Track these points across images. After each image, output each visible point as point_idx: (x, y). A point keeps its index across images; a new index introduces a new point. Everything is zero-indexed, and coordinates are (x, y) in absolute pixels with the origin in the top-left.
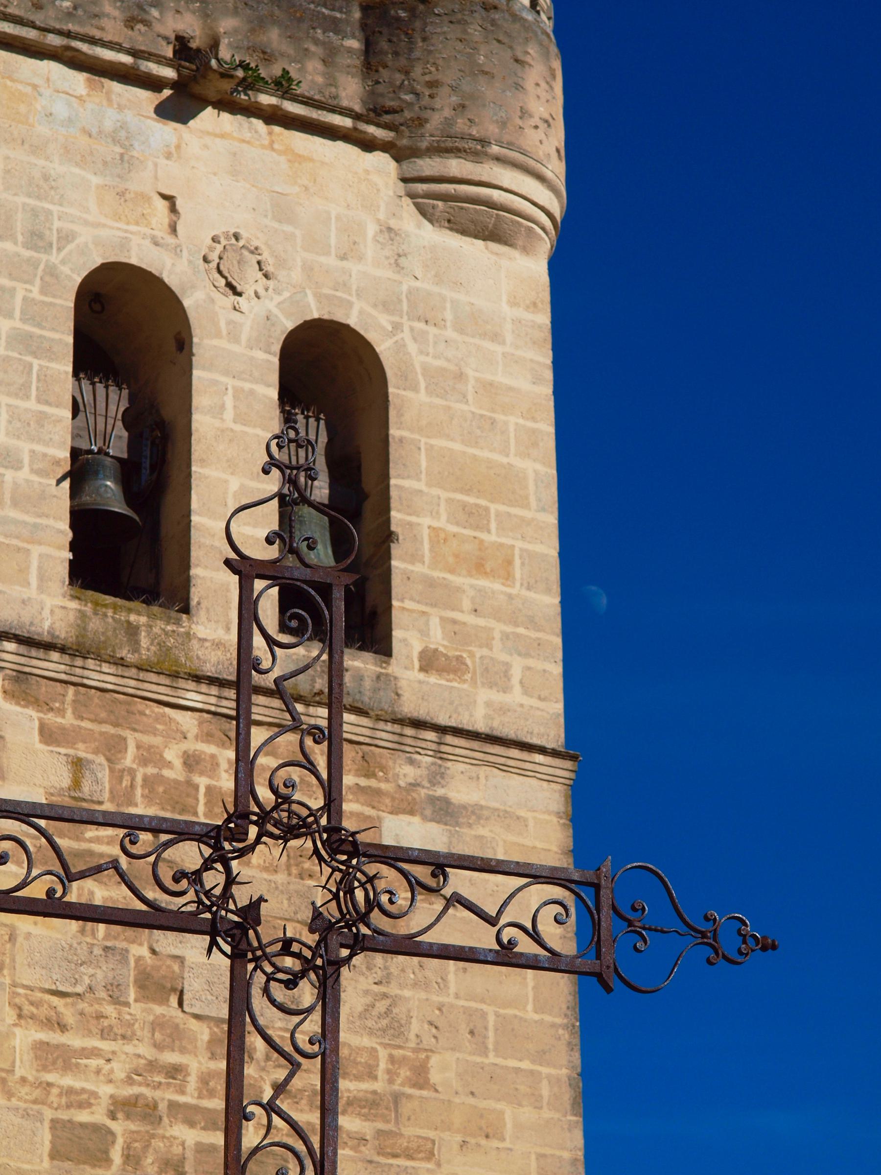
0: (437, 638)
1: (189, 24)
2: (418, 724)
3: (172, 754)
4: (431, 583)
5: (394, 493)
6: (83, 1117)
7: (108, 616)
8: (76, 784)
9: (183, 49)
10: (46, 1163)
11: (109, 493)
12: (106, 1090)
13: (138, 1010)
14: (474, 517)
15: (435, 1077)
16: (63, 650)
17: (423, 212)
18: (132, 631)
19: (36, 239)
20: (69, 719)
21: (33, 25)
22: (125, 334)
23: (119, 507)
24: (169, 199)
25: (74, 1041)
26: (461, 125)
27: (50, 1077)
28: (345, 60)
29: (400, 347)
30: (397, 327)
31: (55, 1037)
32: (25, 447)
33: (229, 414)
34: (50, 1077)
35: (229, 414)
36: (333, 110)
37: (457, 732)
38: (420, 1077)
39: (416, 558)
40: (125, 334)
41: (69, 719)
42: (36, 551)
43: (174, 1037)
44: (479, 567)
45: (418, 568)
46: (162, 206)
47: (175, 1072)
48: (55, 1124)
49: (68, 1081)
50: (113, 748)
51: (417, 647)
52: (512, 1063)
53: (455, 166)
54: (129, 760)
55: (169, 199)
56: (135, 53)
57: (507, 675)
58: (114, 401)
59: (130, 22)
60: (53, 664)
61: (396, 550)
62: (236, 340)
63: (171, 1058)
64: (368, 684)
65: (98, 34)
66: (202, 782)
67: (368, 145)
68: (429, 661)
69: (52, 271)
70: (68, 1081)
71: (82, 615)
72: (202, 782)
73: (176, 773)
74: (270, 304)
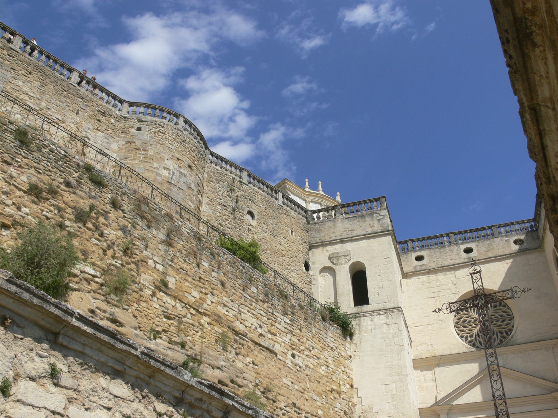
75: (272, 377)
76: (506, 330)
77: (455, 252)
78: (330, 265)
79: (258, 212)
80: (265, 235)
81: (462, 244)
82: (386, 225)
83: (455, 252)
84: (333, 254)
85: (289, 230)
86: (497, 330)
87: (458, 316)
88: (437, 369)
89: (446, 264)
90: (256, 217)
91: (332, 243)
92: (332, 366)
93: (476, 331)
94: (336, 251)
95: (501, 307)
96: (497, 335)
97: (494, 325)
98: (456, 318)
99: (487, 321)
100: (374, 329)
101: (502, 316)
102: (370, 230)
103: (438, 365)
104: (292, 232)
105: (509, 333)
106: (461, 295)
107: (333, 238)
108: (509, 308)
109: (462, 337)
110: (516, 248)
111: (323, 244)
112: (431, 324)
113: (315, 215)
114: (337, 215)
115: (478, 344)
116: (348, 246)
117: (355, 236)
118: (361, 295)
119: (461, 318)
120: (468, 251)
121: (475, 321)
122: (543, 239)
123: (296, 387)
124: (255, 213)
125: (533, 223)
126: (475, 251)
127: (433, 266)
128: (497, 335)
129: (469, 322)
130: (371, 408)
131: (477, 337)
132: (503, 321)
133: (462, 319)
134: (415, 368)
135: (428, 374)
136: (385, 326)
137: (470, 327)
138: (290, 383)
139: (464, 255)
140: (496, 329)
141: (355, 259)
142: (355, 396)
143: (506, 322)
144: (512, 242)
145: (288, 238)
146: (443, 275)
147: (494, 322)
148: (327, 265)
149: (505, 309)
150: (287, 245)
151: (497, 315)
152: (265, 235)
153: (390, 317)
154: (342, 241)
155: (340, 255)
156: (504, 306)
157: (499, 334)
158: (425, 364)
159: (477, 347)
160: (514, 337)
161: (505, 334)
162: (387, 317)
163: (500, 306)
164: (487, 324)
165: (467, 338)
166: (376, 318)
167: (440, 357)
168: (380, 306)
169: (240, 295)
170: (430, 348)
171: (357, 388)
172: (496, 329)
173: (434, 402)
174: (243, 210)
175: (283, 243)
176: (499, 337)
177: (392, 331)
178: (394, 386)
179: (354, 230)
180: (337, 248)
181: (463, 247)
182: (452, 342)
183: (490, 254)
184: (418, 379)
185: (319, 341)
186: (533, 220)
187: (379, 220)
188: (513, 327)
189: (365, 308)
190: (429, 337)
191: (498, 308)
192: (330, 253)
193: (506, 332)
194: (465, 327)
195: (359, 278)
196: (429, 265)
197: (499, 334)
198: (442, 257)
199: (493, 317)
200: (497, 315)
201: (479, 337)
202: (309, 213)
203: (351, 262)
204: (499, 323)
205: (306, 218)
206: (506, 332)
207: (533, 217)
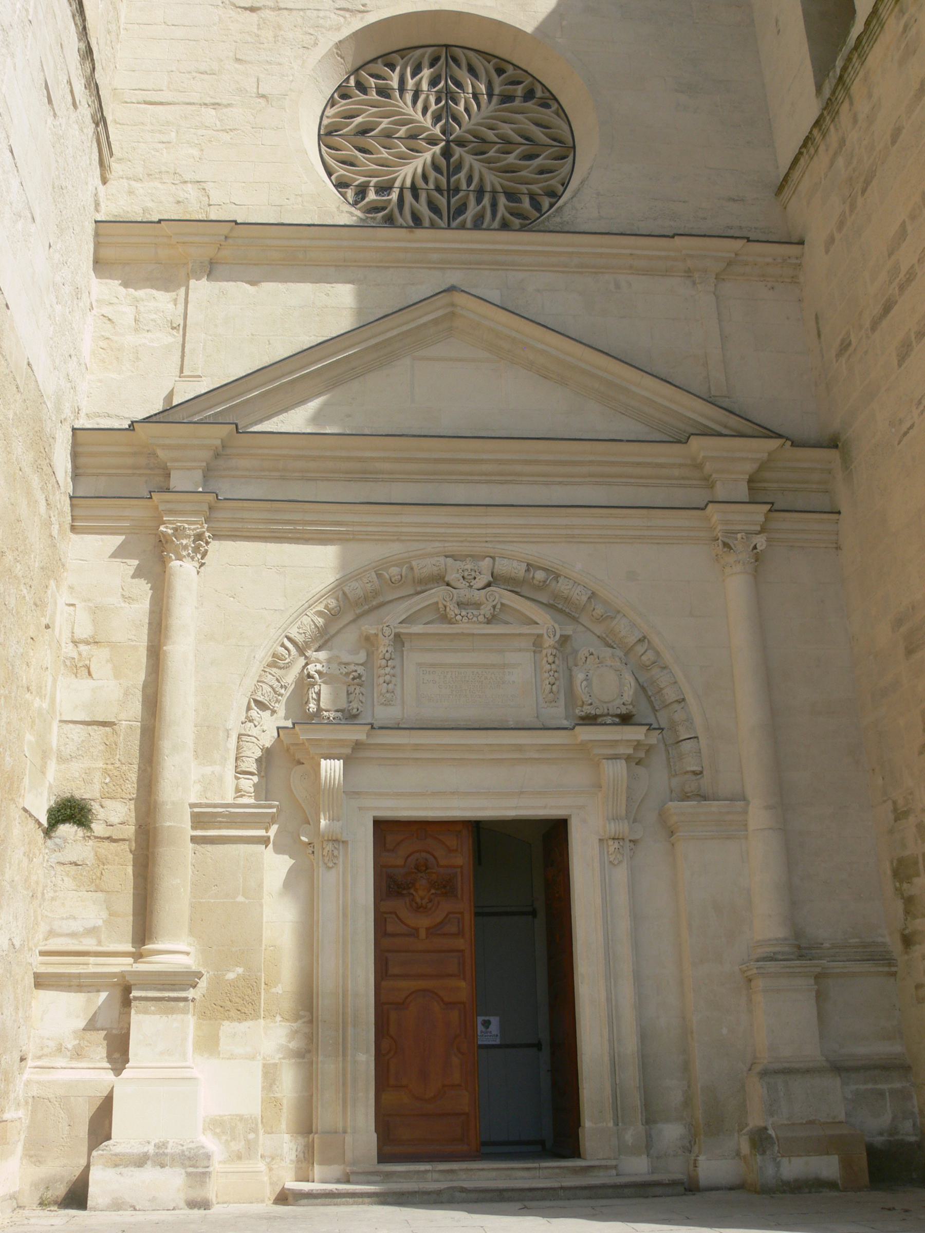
76: (535, 188)
87: (343, 105)
88: (201, 288)
93: (407, 173)
96: (494, 205)
98: (330, 112)
99: (461, 143)
103: (211, 269)
105: (546, 202)
106: (371, 18)
108: (562, 113)
109: (341, 185)
112: (216, 105)
121: (413, 136)
128: (494, 205)
129: (388, 135)
131: (408, 196)
133: (359, 120)
134: (100, 265)
135: (160, 303)
140: (492, 180)
149: (547, 115)
157: (502, 200)
158: (151, 252)
161: (526, 203)
164: (458, 151)
165: (362, 192)
167: (225, 229)
170: (191, 193)
173: (158, 407)
176: (501, 210)
184: (106, 310)
188: (565, 184)
190: (195, 152)
191: (517, 103)
197: (502, 200)
200: (506, 129)
201: (416, 196)
204: (511, 159)
206: (533, 198)
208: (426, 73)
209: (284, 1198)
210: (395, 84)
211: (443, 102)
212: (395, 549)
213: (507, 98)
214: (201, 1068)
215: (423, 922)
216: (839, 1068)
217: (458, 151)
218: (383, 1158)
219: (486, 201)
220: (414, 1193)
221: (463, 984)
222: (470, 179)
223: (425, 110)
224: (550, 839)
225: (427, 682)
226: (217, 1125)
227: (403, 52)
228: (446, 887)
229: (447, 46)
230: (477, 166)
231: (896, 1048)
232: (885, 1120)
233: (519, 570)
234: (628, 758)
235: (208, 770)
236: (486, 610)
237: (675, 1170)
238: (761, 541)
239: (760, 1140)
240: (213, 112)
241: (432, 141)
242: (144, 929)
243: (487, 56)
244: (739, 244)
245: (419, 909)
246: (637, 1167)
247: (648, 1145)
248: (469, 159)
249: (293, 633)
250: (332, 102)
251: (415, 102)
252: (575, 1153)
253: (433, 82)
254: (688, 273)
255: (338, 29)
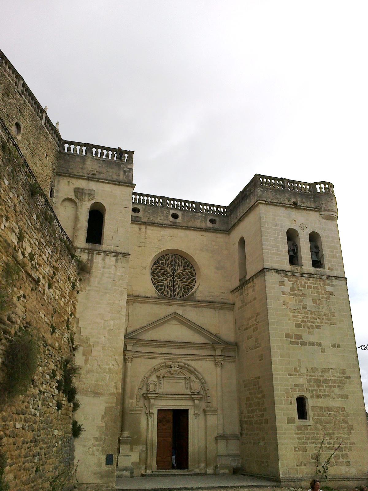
0: (330, 266)
1: (294, 200)
2: (329, 276)
3: (303, 282)
4: (328, 260)
5: (323, 250)
6: (298, 323)
7: (293, 268)
8: (293, 286)
9: (294, 203)
10: (295, 328)
11: (292, 254)
12: (300, 320)
13: (303, 311)
14: (332, 252)
15: (335, 316)
16: (290, 272)
17: (323, 218)
18: (297, 269)
19: (282, 227)
20: (291, 279)
21: (278, 203)
22: (292, 236)
23: (293, 255)
24: (295, 220)
25: (296, 314)
26: (326, 208)
27: (294, 318)
28: (312, 202)
29: (322, 234)
30: (321, 231)
31: (294, 314)
32: (283, 250)
33: (304, 244)
34: (294, 318)
35: (304, 244)
36: (312, 208)
37: (333, 276)
38: (334, 316)
39: (326, 257)
40: (292, 236)
41: (291, 279)
42: (286, 261)
43: (307, 313)
44: (333, 257)
45: (327, 258)
46: (294, 221)
47: (307, 317)
48: (295, 324)
49: (297, 319)
50: (296, 282)
51: (328, 267)
52: (344, 313)
53: (326, 213)
54: (298, 283)
55: (295, 220)
56: (289, 205)
57: (338, 269)
58: (291, 243)
59: (288, 201)
60: (289, 273)
61: (324, 257)
62: (304, 235)
63: (307, 315)
64: (323, 272)
65: (285, 203)
66: (306, 285)
67: (316, 211)
68: (329, 269)
69: (283, 230)
70: (297, 319)
71: (291, 268)
72: (306, 285)
73: (303, 284)
74: (307, 230)
75: (33, 311)
77: (165, 214)
78: (73, 198)
79: (24, 127)
80: (26, 152)
81: (172, 209)
82: (130, 178)
83: (165, 214)
84: (78, 189)
85: (45, 153)
86: (182, 285)
87: (155, 267)
89: (156, 222)
90: (22, 132)
91: (80, 177)
92: (68, 298)
94: (81, 187)
95: (188, 268)
97: (181, 280)
99: (176, 276)
100: (104, 268)
101: (188, 275)
102: (115, 177)
104: (47, 155)
106: (162, 250)
107: (81, 174)
108: (194, 270)
109: (154, 284)
110: (210, 225)
111: (70, 176)
113: (67, 146)
114: (88, 153)
115: (165, 293)
116: (93, 185)
117: (102, 179)
118: (95, 232)
119: (157, 269)
120: (175, 216)
121: (167, 274)
122: (235, 226)
123: (47, 320)
124: (22, 127)
125: (225, 210)
126: (180, 218)
127: (145, 220)
129: (163, 273)
130: (88, 339)
132: (188, 279)
133: (158, 270)
136: (113, 267)
137: (162, 278)
138: (43, 317)
139: (171, 219)
141: (98, 199)
142: (75, 325)
143: (190, 281)
144: (208, 220)
145: (42, 161)
146: (152, 230)
147: (181, 279)
148: (70, 197)
150: (41, 168)
151: (184, 273)
152: (26, 152)
153: (119, 261)
154: (89, 179)
155: (85, 191)
156: (191, 268)
159: (165, 295)
160: (194, 295)
162: (117, 260)
163: (188, 267)
164: (176, 278)
166: (108, 259)
168: (112, 249)
169: (25, 221)
171: (78, 318)
172: (181, 284)
174: (12, 120)
175: (38, 165)
177: (118, 274)
178: (112, 323)
179: (102, 173)
180: (82, 184)
181: (172, 212)
182: (146, 286)
183: (190, 224)
185: (64, 273)
186: (226, 207)
187: (125, 172)
188: (194, 285)
189: (97, 246)
191: (186, 268)
192: (75, 186)
193: (188, 288)
194: (159, 277)
195: (97, 217)
196: (143, 218)
197: (183, 289)
198: (154, 215)
199: (181, 274)
200: (184, 273)
201: (167, 287)
202: (62, 141)
203: (93, 201)
205: (58, 145)
206: (188, 288)
207: (227, 205)
208: (170, 260)
209: (143, 475)
210: (164, 262)
211: (173, 263)
212: (163, 361)
213: (184, 266)
214: (131, 453)
215: (164, 427)
216: (229, 455)
217: (176, 278)
218: (157, 469)
219: (180, 289)
220: (164, 475)
221: (170, 439)
222: (177, 284)
223: (170, 268)
224: (185, 413)
225: (167, 387)
226: (132, 463)
227: (166, 255)
228: (168, 421)
229: (174, 254)
230: (179, 281)
231: (238, 452)
232: (236, 464)
233: (183, 364)
234: (199, 400)
235: (132, 401)
236: (177, 372)
237: (203, 471)
238: (222, 362)
239: (216, 467)
240: (133, 270)
241: (171, 275)
242: (122, 430)
243: (181, 257)
244: (223, 304)
245: (164, 425)
246: (197, 471)
247: (198, 467)
248: (177, 280)
249: (146, 376)
250: (153, 266)
251: (168, 266)
252: (187, 468)
253: (171, 262)
254: (214, 308)
255: (156, 252)
